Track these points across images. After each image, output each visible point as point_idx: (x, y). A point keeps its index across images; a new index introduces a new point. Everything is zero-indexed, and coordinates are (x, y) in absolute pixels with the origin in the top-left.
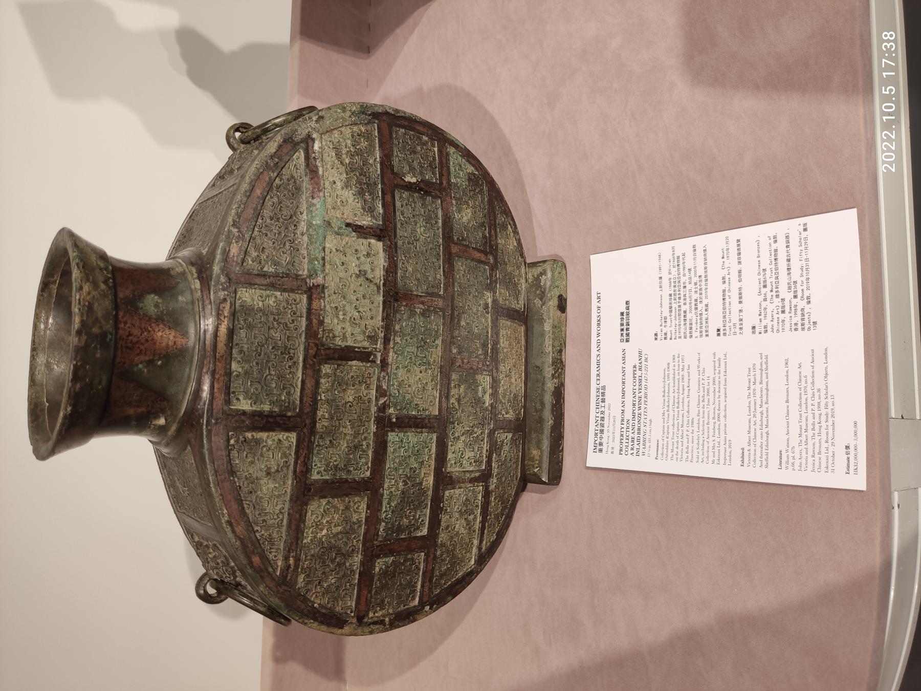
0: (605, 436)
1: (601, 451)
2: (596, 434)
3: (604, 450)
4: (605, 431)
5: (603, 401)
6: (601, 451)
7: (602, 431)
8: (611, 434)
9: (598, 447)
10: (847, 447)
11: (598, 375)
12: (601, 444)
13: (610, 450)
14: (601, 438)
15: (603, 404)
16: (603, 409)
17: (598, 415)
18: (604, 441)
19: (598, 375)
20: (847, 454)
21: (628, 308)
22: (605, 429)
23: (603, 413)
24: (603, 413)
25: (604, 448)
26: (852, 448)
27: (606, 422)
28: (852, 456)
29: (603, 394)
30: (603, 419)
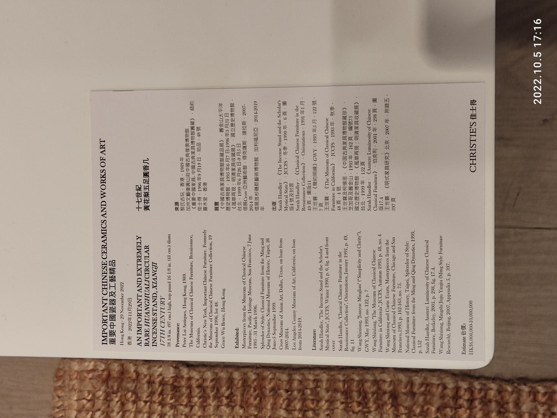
0: (118, 322)
1: (113, 341)
2: (104, 322)
4: (118, 317)
5: (113, 279)
6: (113, 341)
7: (113, 318)
8: (126, 321)
10: (463, 327)
12: (112, 333)
13: (126, 340)
14: (112, 326)
15: (112, 284)
16: (112, 289)
18: (117, 329)
20: (463, 334)
22: (118, 314)
23: (113, 294)
25: (118, 337)
26: (468, 327)
27: (118, 306)
28: (467, 336)
29: (112, 271)
30: (113, 302)
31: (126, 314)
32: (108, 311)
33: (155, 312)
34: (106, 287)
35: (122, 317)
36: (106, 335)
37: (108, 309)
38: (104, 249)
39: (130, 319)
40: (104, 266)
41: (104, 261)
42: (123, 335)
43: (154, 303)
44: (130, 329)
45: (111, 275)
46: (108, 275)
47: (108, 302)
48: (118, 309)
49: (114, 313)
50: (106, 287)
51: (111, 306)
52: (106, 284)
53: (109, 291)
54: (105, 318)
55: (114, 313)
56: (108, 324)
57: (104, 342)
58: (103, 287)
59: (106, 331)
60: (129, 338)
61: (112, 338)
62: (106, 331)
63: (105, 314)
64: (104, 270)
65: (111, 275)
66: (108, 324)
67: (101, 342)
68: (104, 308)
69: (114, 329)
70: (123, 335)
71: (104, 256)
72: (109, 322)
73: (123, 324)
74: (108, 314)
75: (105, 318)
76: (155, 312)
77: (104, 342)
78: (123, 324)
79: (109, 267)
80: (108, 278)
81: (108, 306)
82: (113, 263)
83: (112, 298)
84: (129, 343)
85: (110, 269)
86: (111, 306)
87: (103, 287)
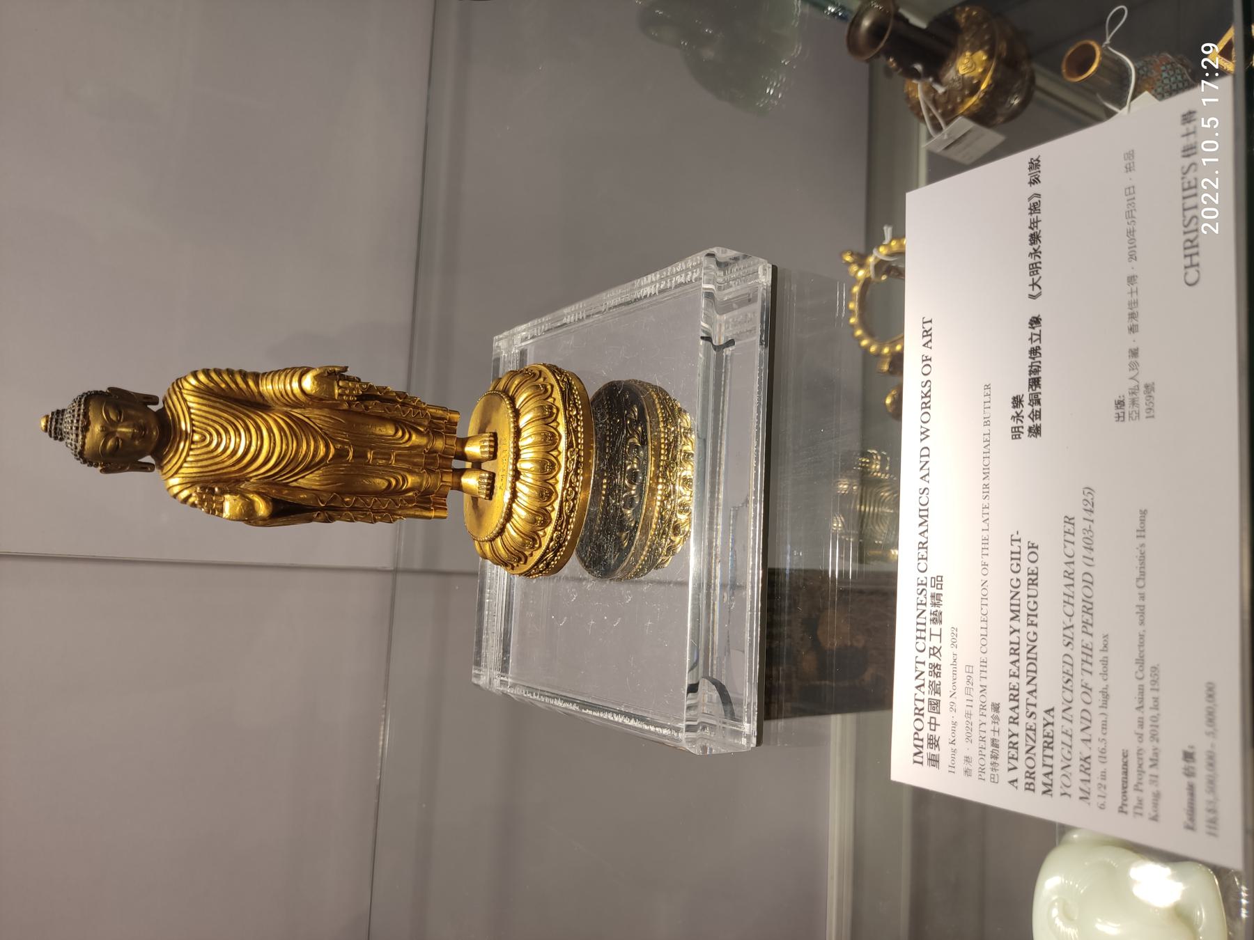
0: (944, 718)
1: (934, 761)
2: (919, 712)
3: (945, 759)
4: (944, 706)
5: (937, 619)
6: (934, 761)
7: (934, 706)
8: (960, 718)
9: (926, 751)
11: (923, 545)
12: (933, 742)
13: (960, 765)
14: (934, 724)
15: (936, 629)
16: (935, 642)
17: (924, 657)
18: (943, 733)
19: (923, 545)
21: (1035, 382)
22: (944, 699)
23: (935, 652)
24: (935, 652)
25: (944, 752)
27: (945, 680)
29: (937, 599)
30: (936, 669)
31: (961, 700)
32: (926, 689)
33: (1032, 709)
34: (923, 634)
35: (952, 708)
36: (919, 743)
37: (927, 684)
38: (923, 552)
39: (968, 715)
40: (921, 587)
41: (922, 576)
42: (954, 751)
43: (1031, 688)
44: (968, 739)
45: (934, 609)
46: (929, 608)
47: (926, 669)
48: (946, 688)
49: (937, 697)
50: (923, 634)
51: (932, 679)
52: (922, 627)
53: (929, 644)
54: (920, 705)
55: (937, 697)
56: (926, 719)
57: (917, 758)
58: (918, 634)
59: (922, 735)
60: (967, 759)
61: (933, 752)
62: (922, 735)
63: (920, 696)
64: (922, 597)
65: (934, 609)
66: (926, 719)
67: (911, 758)
68: (919, 682)
69: (937, 734)
70: (954, 751)
71: (922, 567)
72: (927, 715)
73: (955, 724)
74: (926, 697)
75: (920, 705)
76: (1032, 709)
77: (917, 758)
78: (955, 724)
79: (930, 590)
80: (927, 614)
81: (925, 676)
82: (938, 581)
83: (934, 660)
84: (967, 772)
85: (932, 596)
86: (932, 679)
87: (918, 634)
